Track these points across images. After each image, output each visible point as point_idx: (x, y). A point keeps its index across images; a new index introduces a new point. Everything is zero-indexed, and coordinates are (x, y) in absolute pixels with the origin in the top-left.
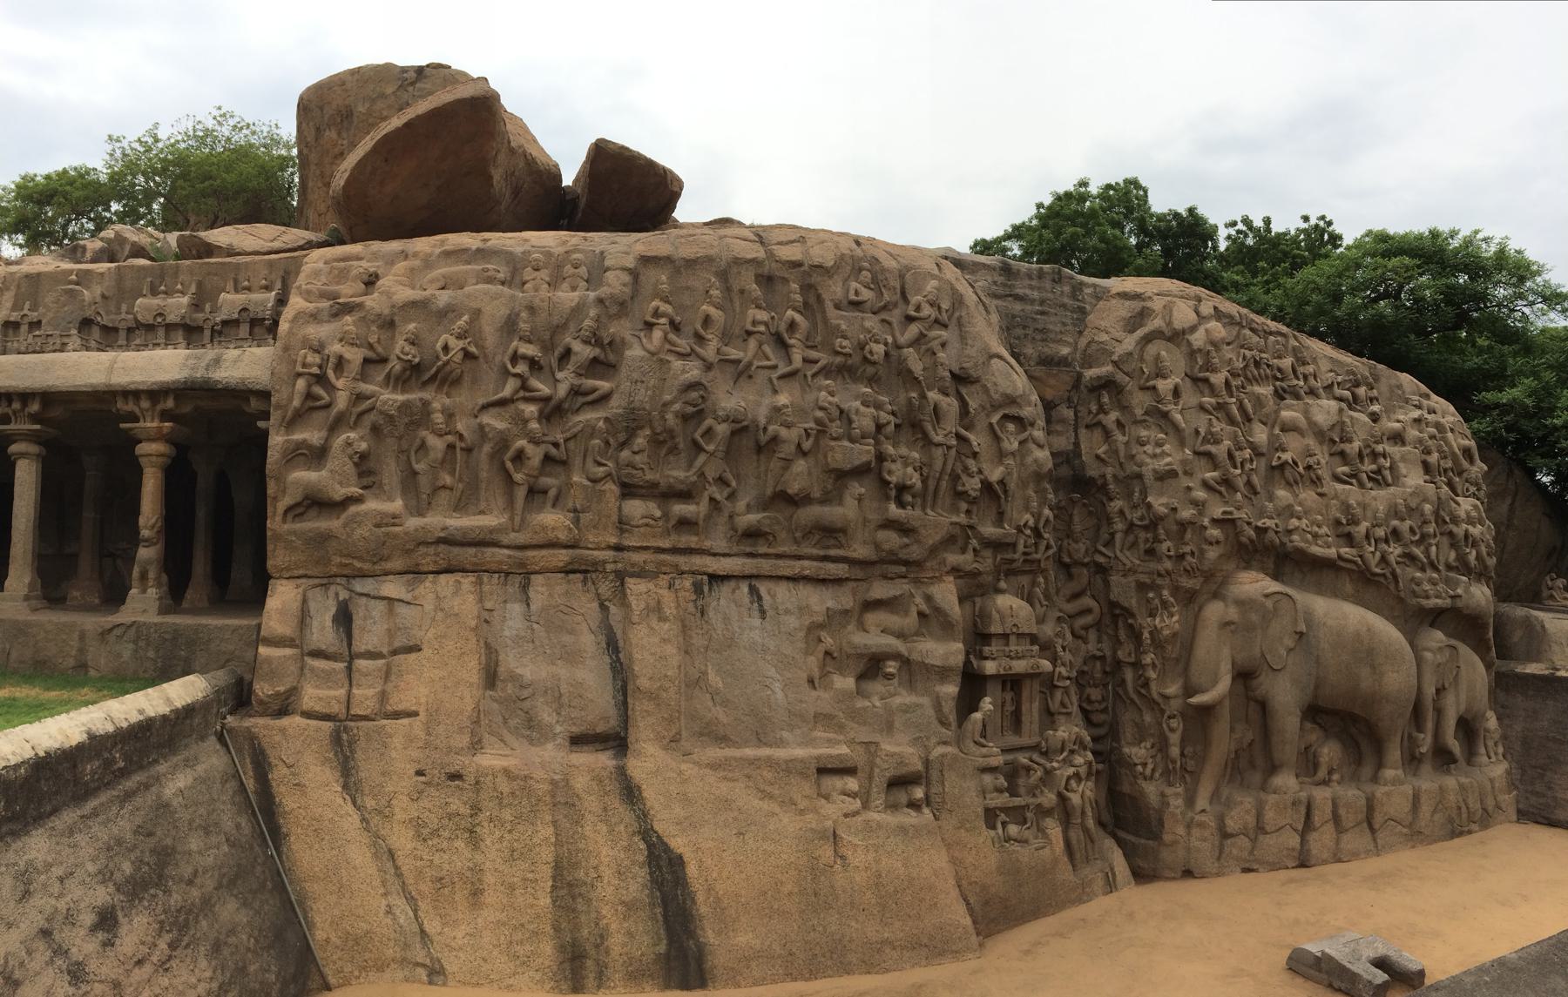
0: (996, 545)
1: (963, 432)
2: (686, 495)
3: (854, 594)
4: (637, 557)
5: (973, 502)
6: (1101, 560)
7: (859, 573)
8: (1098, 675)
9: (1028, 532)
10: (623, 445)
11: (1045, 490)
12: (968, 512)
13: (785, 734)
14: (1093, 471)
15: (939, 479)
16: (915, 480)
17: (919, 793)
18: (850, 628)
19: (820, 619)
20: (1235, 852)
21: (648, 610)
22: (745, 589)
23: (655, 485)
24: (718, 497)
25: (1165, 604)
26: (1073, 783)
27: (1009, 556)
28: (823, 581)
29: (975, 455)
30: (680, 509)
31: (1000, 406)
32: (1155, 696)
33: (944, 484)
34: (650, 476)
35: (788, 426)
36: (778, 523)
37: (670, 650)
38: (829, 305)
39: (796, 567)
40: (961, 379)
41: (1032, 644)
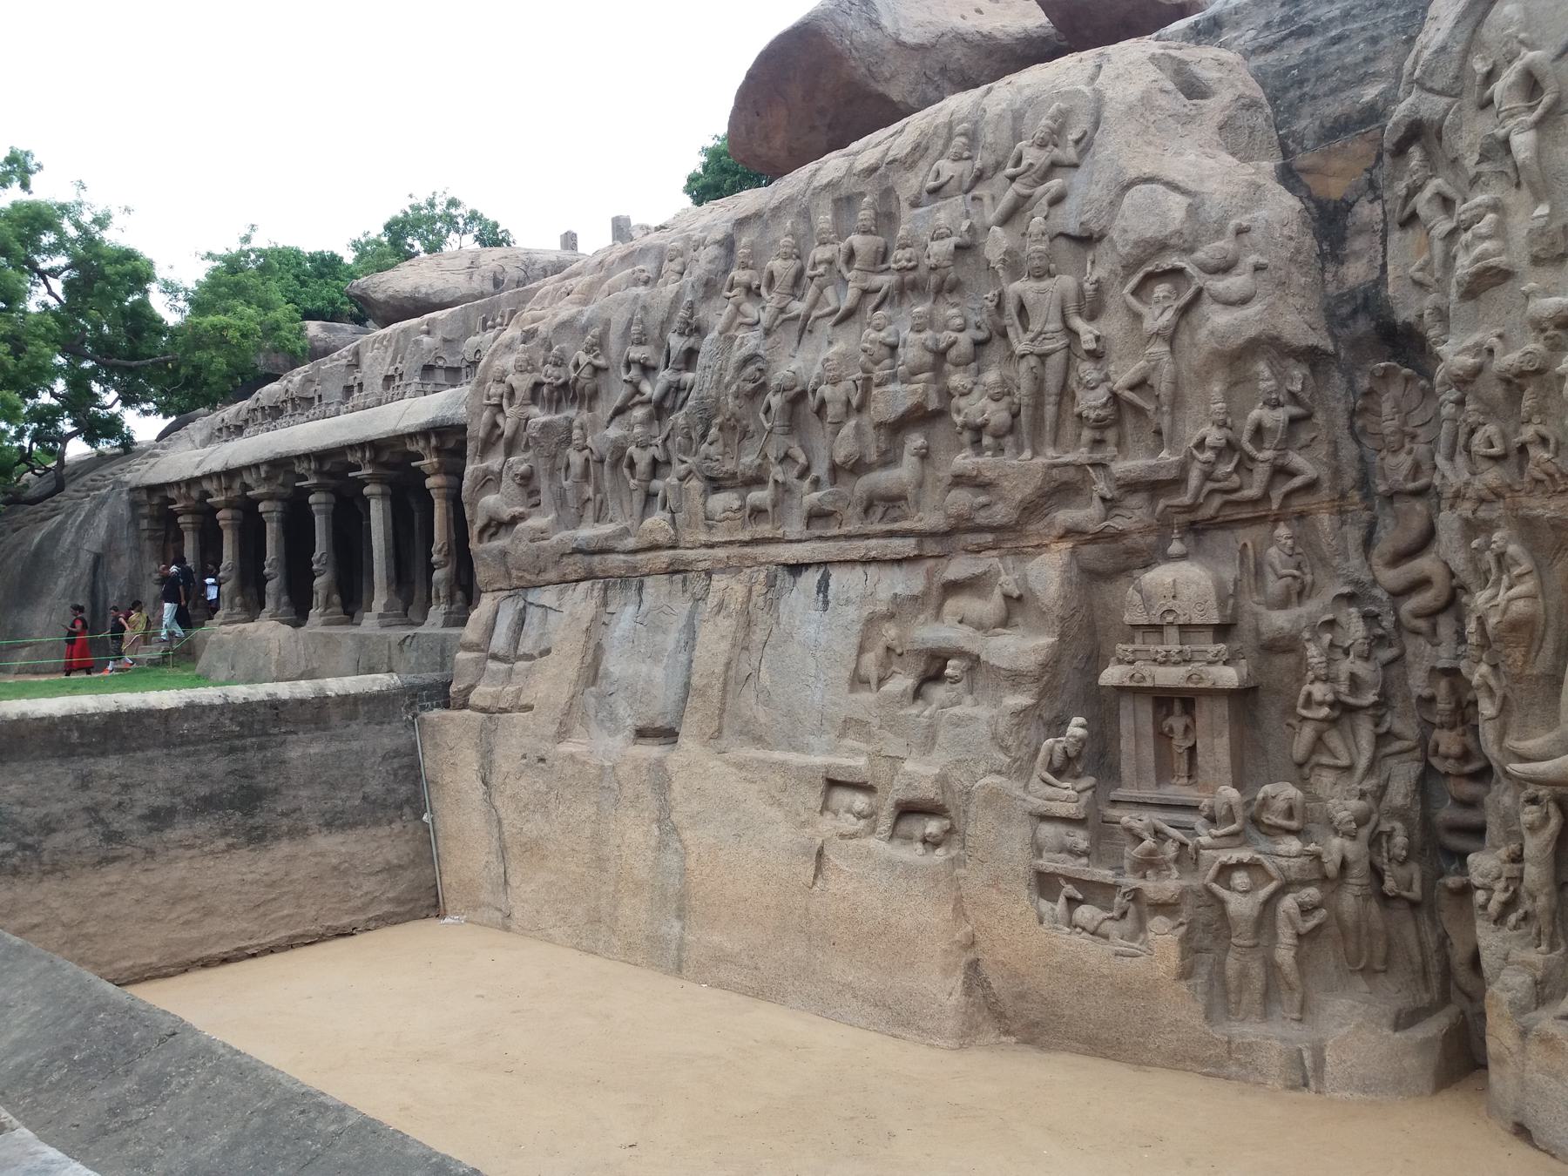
0: (1153, 487)
1: (1078, 323)
2: (757, 481)
3: (930, 575)
4: (721, 553)
5: (1100, 425)
6: (1437, 481)
7: (931, 547)
8: (1443, 705)
9: (1209, 455)
10: (704, 436)
11: (1256, 377)
12: (1098, 443)
13: (812, 739)
14: (1404, 315)
15: (1038, 405)
16: (997, 414)
17: (933, 827)
18: (922, 618)
19: (882, 608)
21: (721, 606)
22: (818, 576)
23: (734, 475)
24: (780, 478)
26: (1240, 879)
27: (1176, 501)
28: (898, 562)
29: (1095, 356)
30: (759, 496)
31: (1140, 263)
33: (1050, 411)
34: (729, 466)
35: (835, 382)
36: (842, 498)
37: (724, 646)
38: (905, 205)
39: (858, 549)
40: (1086, 240)
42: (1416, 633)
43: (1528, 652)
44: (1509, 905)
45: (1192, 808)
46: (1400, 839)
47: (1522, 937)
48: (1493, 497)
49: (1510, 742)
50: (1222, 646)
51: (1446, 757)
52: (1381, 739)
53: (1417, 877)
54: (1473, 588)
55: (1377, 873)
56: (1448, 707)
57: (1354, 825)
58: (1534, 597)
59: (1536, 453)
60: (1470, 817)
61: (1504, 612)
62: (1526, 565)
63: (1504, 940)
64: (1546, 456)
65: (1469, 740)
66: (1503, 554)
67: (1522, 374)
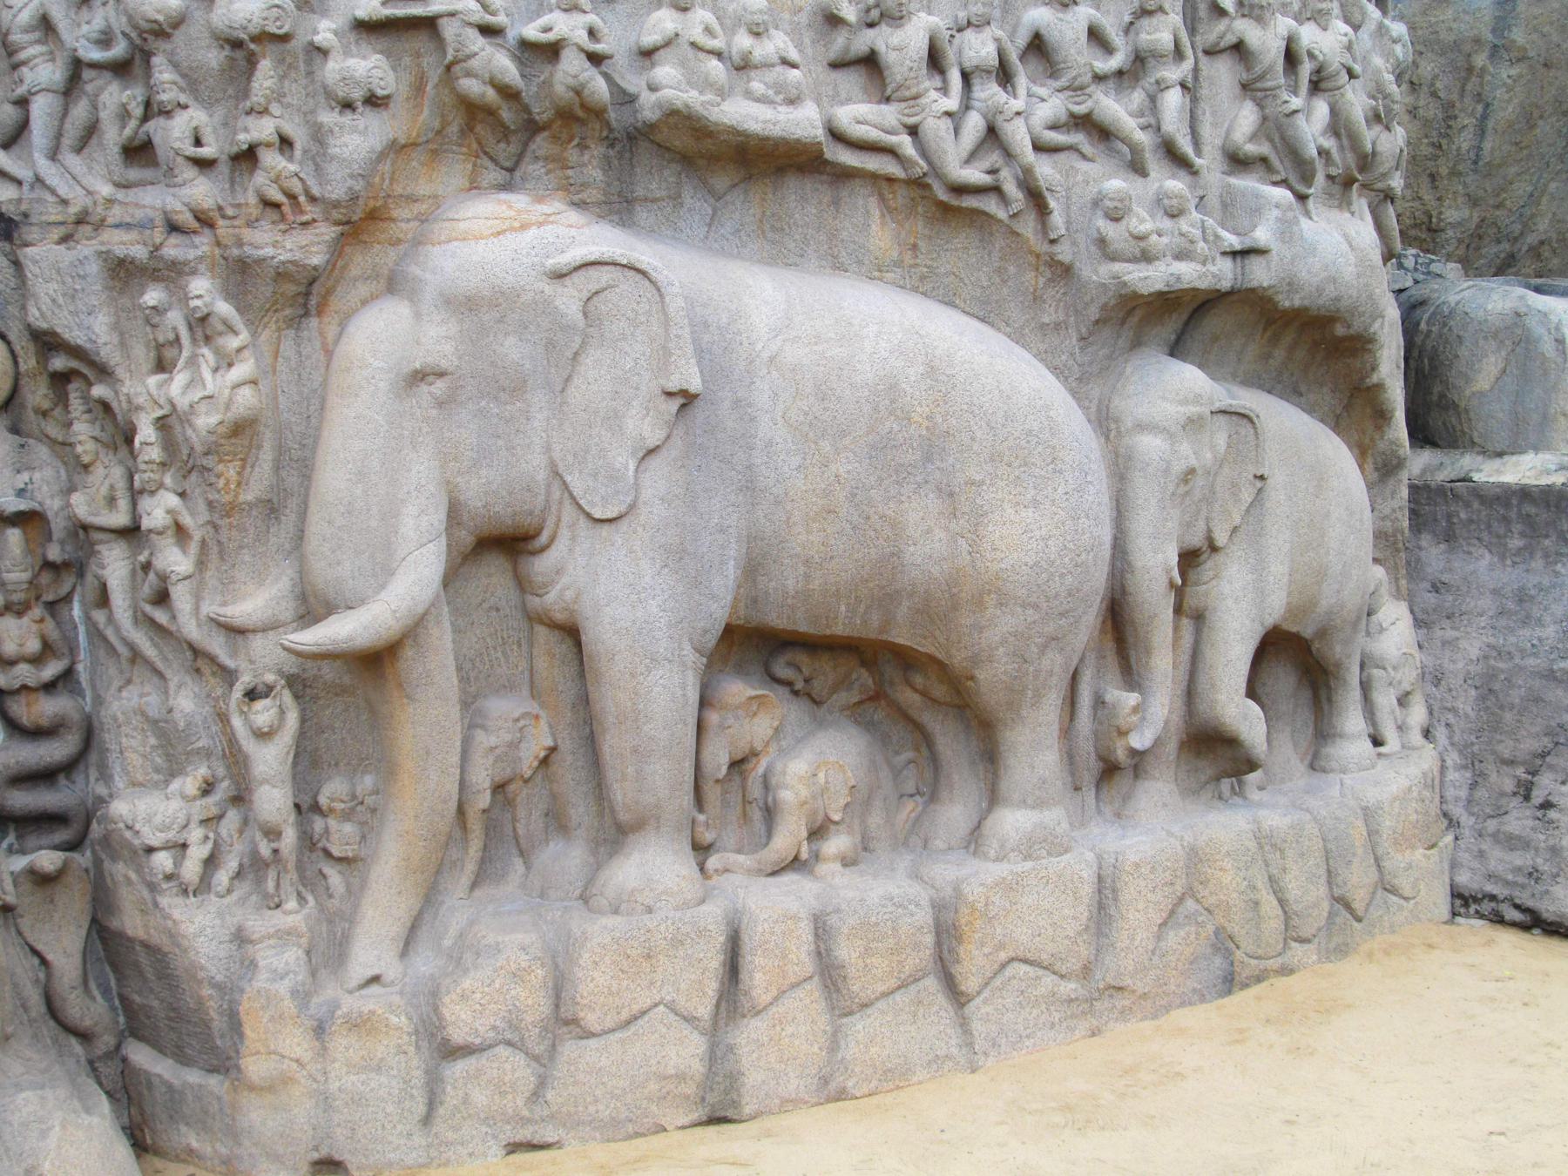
20: (480, 1097)
25: (202, 325)
32: (191, 629)
43: (243, 467)
44: (211, 862)
47: (242, 901)
48: (195, 225)
49: (209, 608)
51: (12, 663)
54: (120, 372)
56: (26, 576)
58: (254, 382)
59: (272, 160)
61: (228, 407)
62: (244, 336)
63: (220, 915)
64: (293, 167)
65: (50, 625)
66: (204, 319)
67: (263, 37)
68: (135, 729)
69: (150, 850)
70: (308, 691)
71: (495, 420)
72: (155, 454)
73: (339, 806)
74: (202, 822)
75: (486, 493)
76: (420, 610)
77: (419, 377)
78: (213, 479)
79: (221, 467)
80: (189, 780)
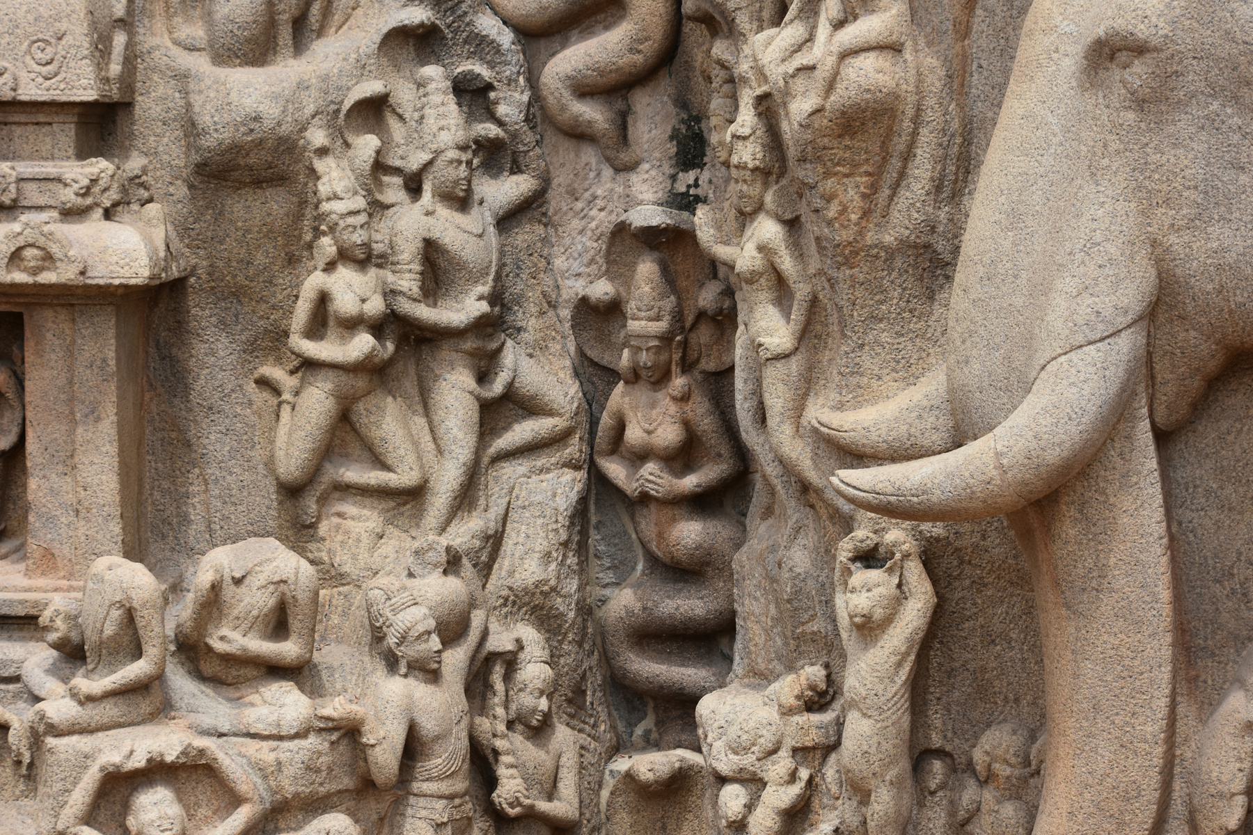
41: (83, 153)
42: (579, 135)
43: (874, 188)
45: (21, 623)
46: (534, 671)
49: (819, 412)
50: (100, 166)
51: (640, 456)
52: (497, 411)
53: (569, 761)
54: (743, 21)
55: (482, 764)
57: (435, 643)
60: (688, 605)
61: (830, 86)
65: (700, 410)
68: (758, 586)
69: (722, 780)
70: (968, 570)
71: (1236, 138)
72: (749, 154)
73: (1002, 770)
74: (795, 751)
75: (1219, 267)
76: (1053, 456)
77: (1108, 53)
78: (818, 203)
79: (830, 183)
80: (790, 678)
